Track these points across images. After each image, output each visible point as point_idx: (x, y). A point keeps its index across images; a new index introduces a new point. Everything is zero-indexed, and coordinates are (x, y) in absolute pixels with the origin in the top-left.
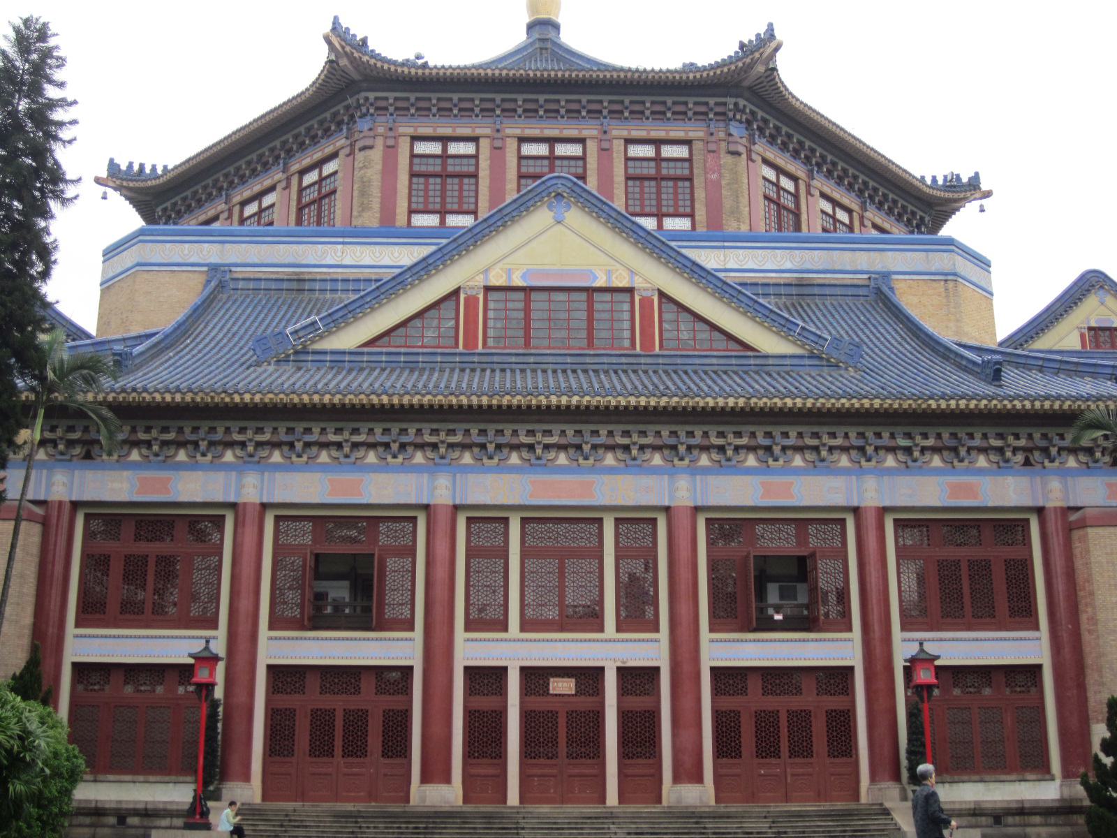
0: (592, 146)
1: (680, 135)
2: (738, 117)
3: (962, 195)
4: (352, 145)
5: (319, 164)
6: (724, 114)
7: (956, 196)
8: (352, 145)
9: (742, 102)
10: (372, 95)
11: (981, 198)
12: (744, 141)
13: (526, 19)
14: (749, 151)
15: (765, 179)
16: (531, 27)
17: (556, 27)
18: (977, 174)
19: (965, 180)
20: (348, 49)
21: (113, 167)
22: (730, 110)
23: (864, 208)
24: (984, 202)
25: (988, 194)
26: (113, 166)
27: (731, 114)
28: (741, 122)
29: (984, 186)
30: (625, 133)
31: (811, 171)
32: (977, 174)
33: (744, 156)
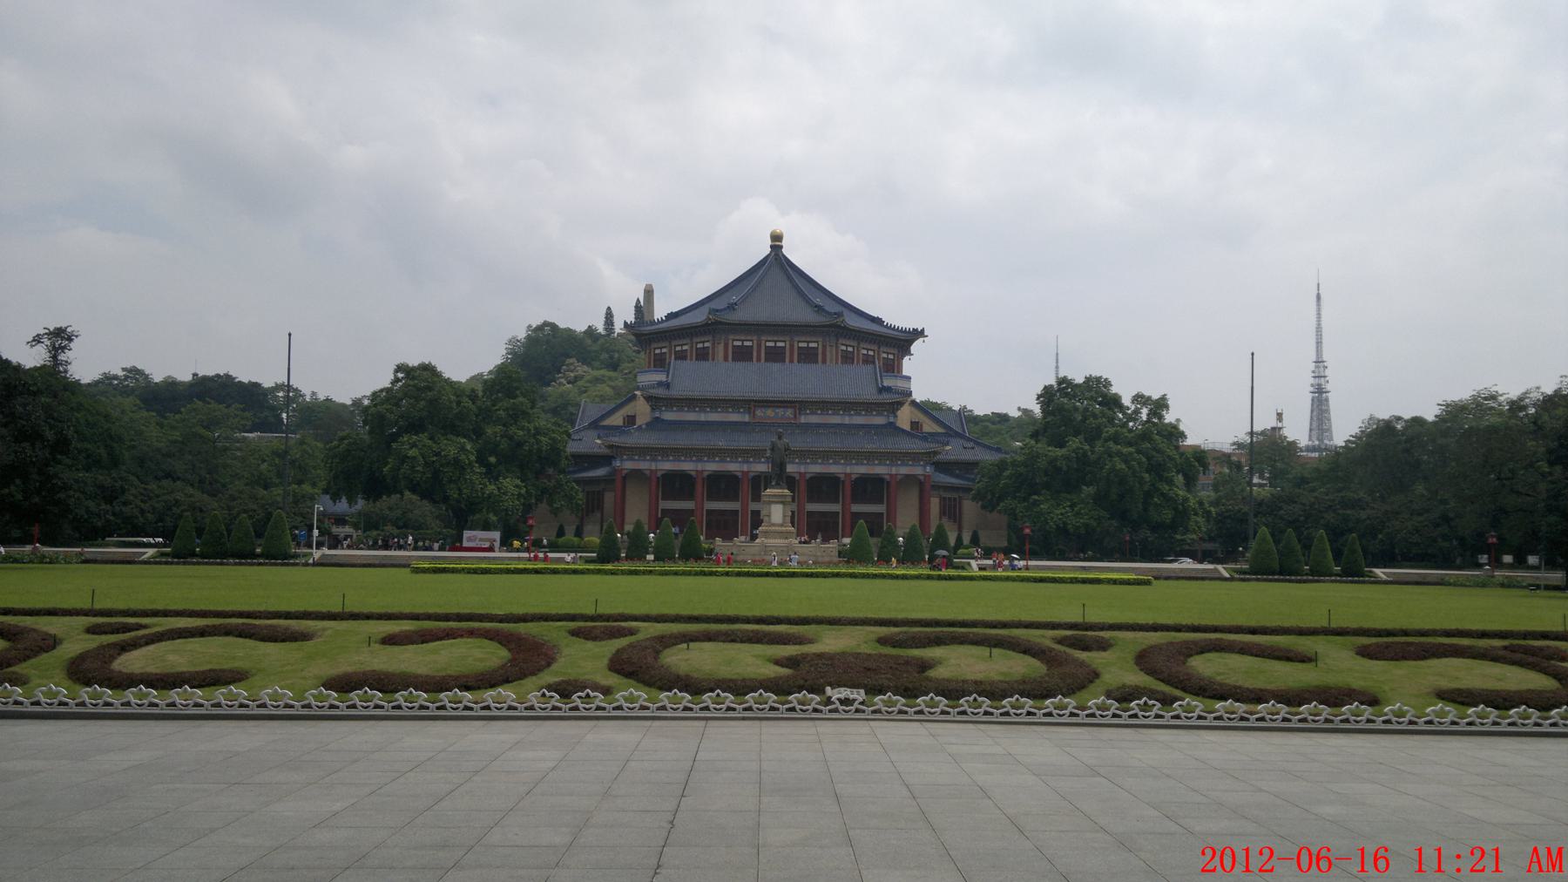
0: (788, 343)
1: (814, 340)
4: (714, 341)
5: (703, 342)
8: (714, 341)
10: (720, 326)
13: (770, 243)
14: (836, 344)
15: (842, 350)
16: (771, 247)
17: (781, 247)
21: (625, 323)
23: (879, 348)
24: (925, 339)
25: (927, 336)
26: (625, 323)
33: (834, 348)
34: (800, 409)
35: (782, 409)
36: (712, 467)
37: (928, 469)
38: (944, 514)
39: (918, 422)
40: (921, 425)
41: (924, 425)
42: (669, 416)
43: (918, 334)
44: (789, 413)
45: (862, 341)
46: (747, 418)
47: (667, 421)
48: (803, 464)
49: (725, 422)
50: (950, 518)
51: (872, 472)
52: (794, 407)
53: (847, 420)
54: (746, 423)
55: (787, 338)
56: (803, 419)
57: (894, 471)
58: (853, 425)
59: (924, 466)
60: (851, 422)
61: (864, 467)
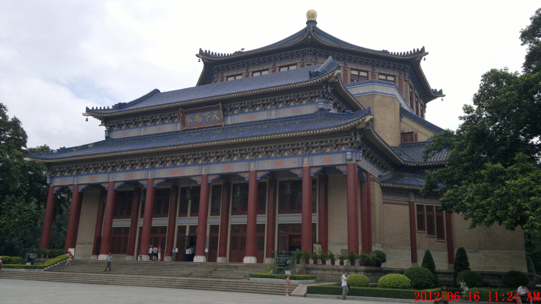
2: (309, 53)
3: (417, 56)
6: (305, 53)
7: (414, 57)
9: (309, 48)
11: (424, 56)
12: (313, 60)
13: (306, 20)
18: (423, 47)
19: (420, 50)
20: (204, 57)
22: (307, 52)
24: (426, 57)
25: (427, 54)
27: (307, 53)
28: (311, 54)
29: (426, 51)
30: (279, 65)
31: (345, 63)
32: (423, 47)
34: (224, 110)
35: (209, 113)
36: (121, 177)
37: (349, 155)
38: (421, 227)
39: (412, 133)
40: (416, 135)
41: (419, 134)
42: (117, 135)
43: (421, 53)
44: (215, 116)
45: (349, 60)
46: (179, 127)
47: (115, 139)
48: (205, 164)
49: (160, 134)
50: (431, 232)
51: (279, 167)
52: (218, 108)
53: (273, 114)
54: (178, 132)
55: (270, 66)
56: (230, 121)
57: (306, 162)
58: (279, 119)
59: (345, 152)
60: (277, 117)
61: (270, 161)
